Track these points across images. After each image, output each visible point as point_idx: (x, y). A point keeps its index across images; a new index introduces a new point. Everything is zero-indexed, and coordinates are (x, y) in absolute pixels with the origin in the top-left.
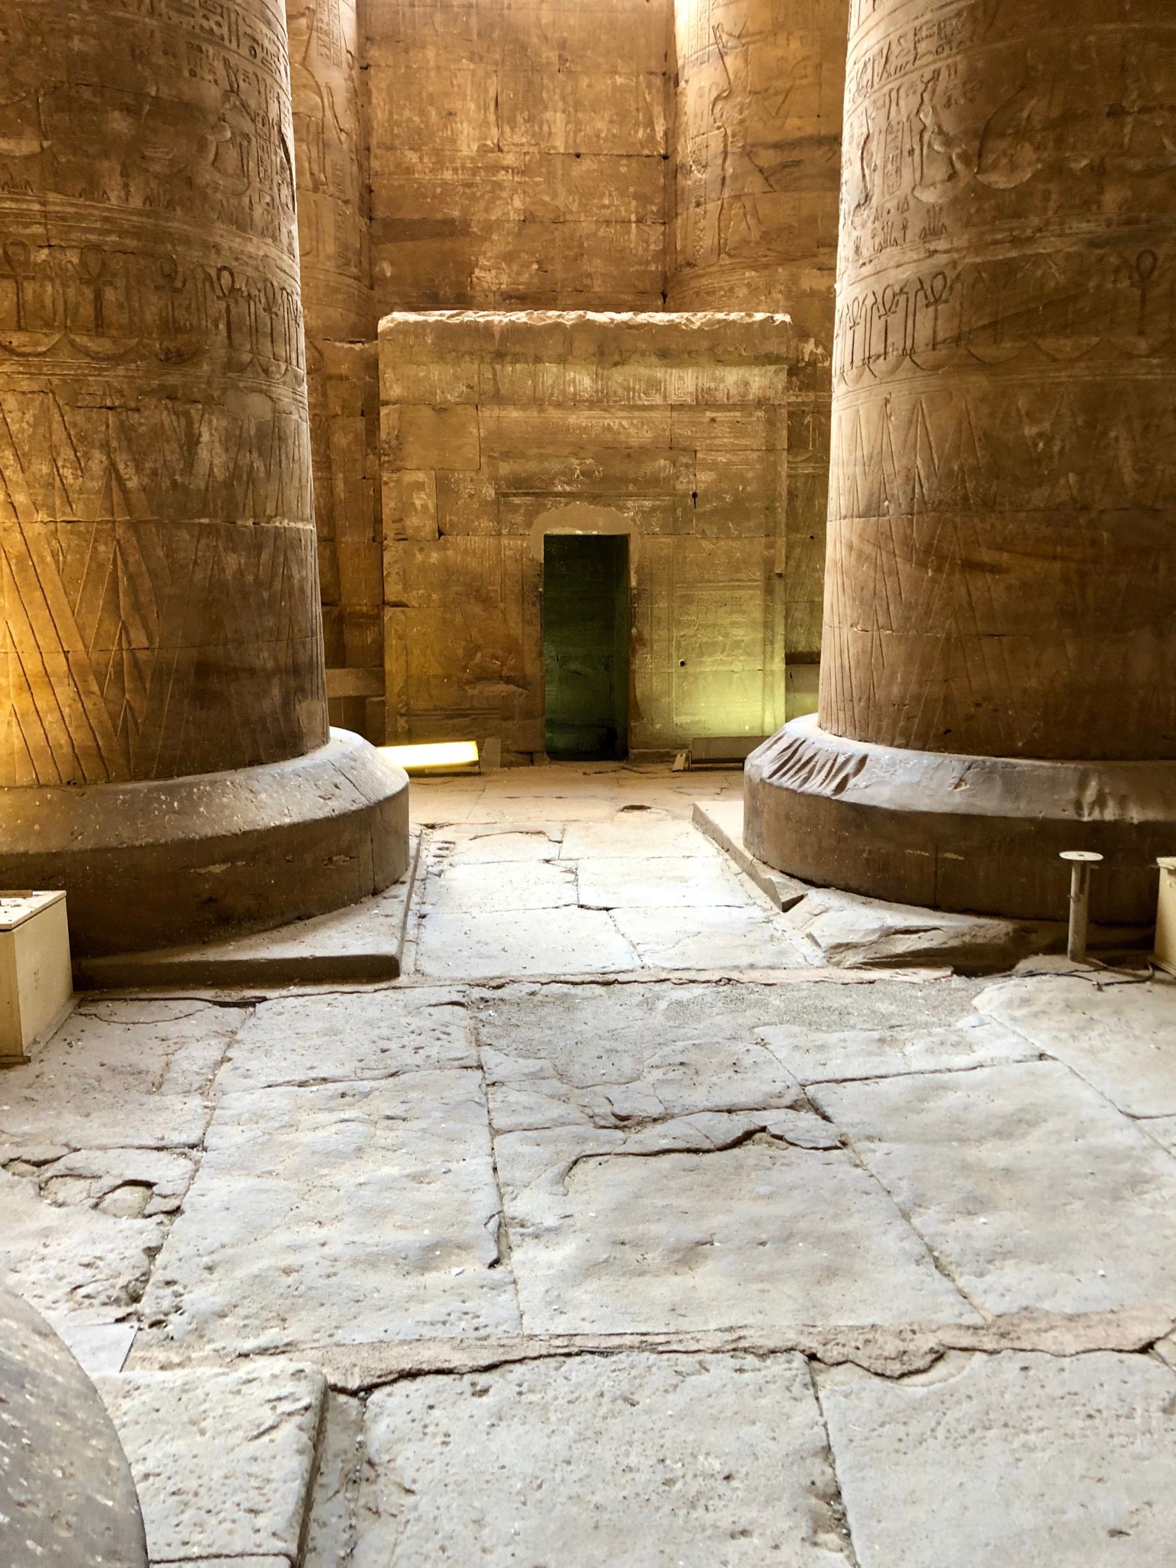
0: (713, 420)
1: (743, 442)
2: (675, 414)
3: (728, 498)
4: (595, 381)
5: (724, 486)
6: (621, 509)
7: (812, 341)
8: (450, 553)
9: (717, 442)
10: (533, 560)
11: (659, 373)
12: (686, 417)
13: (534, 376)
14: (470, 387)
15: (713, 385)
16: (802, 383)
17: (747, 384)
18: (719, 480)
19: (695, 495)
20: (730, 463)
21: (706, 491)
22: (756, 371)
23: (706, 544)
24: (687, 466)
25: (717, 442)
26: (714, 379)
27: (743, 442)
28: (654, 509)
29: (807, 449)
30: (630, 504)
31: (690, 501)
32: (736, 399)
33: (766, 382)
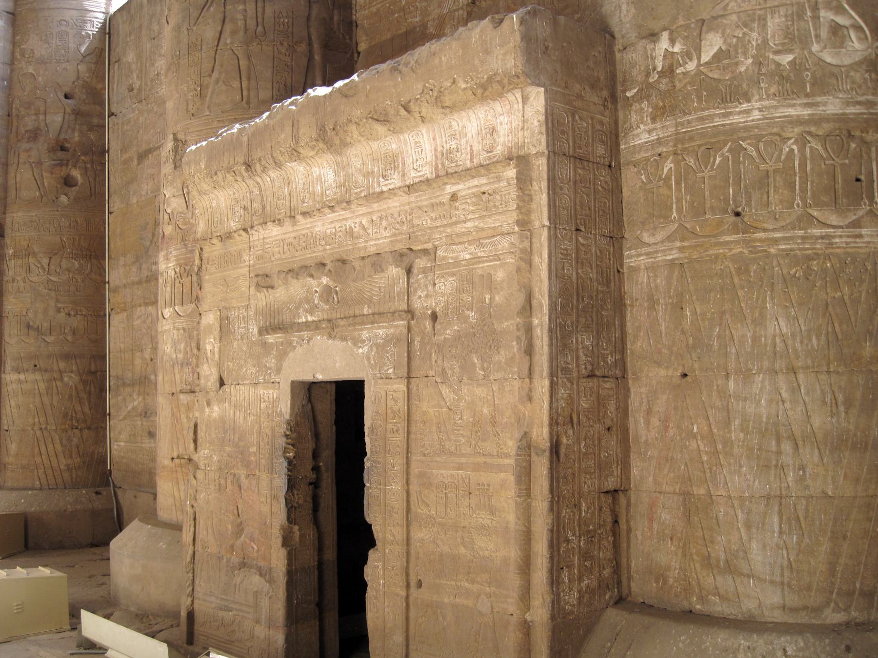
0: (454, 197)
1: (490, 223)
2: (413, 198)
3: (472, 315)
4: (337, 174)
5: (467, 298)
6: (357, 342)
7: (665, 35)
8: (227, 405)
9: (459, 229)
10: (281, 414)
11: (392, 144)
12: (423, 198)
13: (288, 181)
14: (245, 208)
15: (453, 144)
16: (656, 108)
17: (493, 131)
18: (459, 290)
19: (434, 317)
20: (476, 260)
21: (446, 308)
22: (498, 106)
23: (445, 390)
24: (425, 271)
25: (459, 229)
26: (453, 136)
27: (490, 223)
28: (388, 340)
29: (667, 217)
30: (365, 335)
31: (428, 324)
32: (482, 157)
33: (516, 122)
